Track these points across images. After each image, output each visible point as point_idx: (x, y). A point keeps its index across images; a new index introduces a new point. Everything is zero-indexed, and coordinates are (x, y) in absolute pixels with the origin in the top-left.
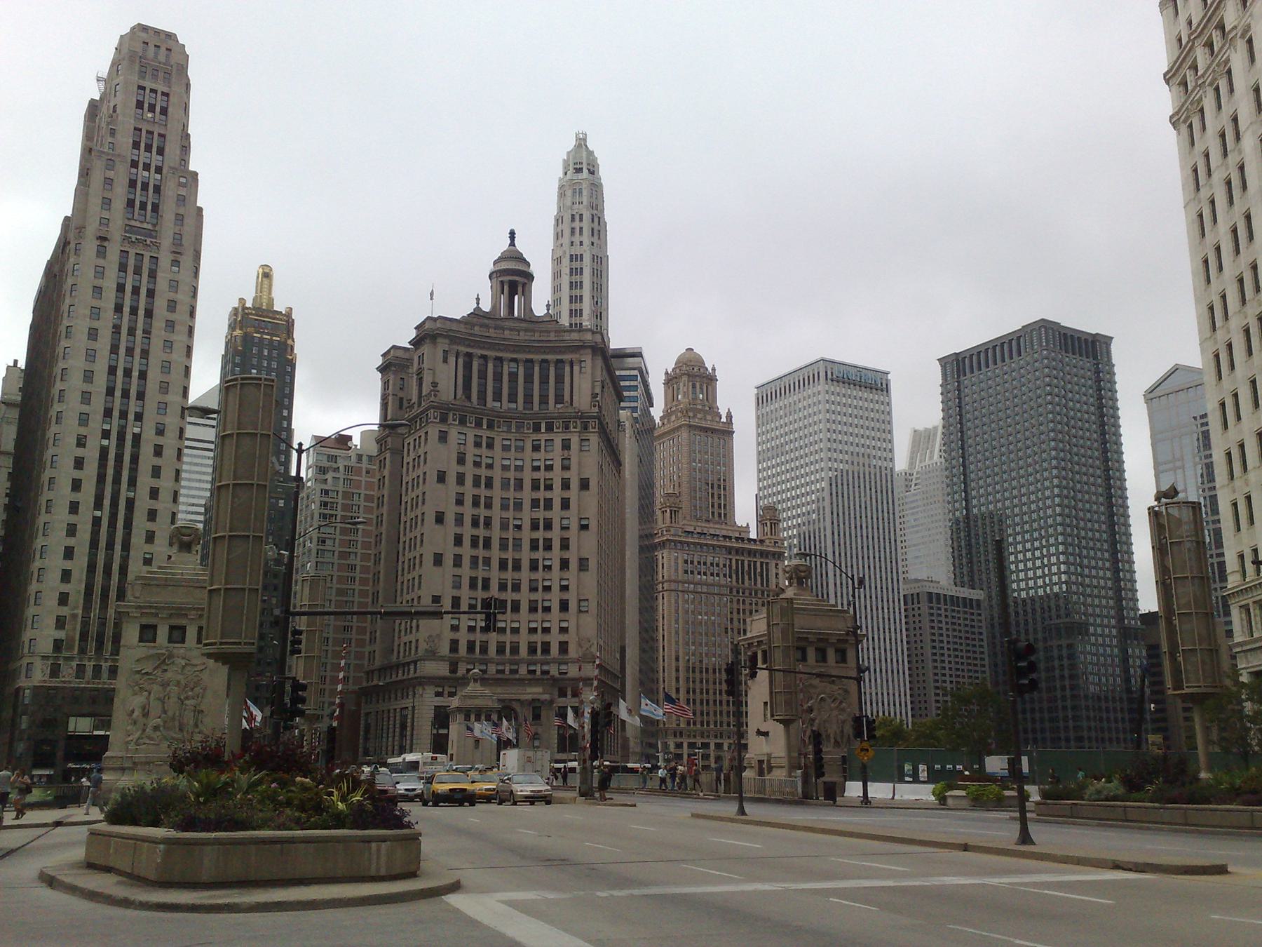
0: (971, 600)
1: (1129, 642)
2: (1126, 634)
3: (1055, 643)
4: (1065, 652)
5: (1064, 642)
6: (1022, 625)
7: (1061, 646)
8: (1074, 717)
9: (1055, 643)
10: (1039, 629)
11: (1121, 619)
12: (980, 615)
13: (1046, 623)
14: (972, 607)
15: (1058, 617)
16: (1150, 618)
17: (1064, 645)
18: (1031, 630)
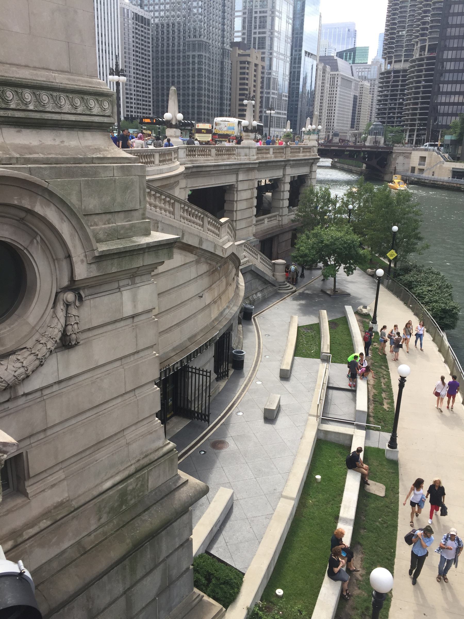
0: (145, 18)
2: (224, 53)
3: (191, 53)
4: (196, 60)
5: (196, 53)
6: (171, 40)
7: (194, 55)
9: (191, 53)
10: (182, 43)
11: (223, 43)
12: (149, 30)
13: (187, 40)
14: (145, 25)
15: (195, 36)
16: (234, 44)
17: (197, 55)
18: (176, 44)
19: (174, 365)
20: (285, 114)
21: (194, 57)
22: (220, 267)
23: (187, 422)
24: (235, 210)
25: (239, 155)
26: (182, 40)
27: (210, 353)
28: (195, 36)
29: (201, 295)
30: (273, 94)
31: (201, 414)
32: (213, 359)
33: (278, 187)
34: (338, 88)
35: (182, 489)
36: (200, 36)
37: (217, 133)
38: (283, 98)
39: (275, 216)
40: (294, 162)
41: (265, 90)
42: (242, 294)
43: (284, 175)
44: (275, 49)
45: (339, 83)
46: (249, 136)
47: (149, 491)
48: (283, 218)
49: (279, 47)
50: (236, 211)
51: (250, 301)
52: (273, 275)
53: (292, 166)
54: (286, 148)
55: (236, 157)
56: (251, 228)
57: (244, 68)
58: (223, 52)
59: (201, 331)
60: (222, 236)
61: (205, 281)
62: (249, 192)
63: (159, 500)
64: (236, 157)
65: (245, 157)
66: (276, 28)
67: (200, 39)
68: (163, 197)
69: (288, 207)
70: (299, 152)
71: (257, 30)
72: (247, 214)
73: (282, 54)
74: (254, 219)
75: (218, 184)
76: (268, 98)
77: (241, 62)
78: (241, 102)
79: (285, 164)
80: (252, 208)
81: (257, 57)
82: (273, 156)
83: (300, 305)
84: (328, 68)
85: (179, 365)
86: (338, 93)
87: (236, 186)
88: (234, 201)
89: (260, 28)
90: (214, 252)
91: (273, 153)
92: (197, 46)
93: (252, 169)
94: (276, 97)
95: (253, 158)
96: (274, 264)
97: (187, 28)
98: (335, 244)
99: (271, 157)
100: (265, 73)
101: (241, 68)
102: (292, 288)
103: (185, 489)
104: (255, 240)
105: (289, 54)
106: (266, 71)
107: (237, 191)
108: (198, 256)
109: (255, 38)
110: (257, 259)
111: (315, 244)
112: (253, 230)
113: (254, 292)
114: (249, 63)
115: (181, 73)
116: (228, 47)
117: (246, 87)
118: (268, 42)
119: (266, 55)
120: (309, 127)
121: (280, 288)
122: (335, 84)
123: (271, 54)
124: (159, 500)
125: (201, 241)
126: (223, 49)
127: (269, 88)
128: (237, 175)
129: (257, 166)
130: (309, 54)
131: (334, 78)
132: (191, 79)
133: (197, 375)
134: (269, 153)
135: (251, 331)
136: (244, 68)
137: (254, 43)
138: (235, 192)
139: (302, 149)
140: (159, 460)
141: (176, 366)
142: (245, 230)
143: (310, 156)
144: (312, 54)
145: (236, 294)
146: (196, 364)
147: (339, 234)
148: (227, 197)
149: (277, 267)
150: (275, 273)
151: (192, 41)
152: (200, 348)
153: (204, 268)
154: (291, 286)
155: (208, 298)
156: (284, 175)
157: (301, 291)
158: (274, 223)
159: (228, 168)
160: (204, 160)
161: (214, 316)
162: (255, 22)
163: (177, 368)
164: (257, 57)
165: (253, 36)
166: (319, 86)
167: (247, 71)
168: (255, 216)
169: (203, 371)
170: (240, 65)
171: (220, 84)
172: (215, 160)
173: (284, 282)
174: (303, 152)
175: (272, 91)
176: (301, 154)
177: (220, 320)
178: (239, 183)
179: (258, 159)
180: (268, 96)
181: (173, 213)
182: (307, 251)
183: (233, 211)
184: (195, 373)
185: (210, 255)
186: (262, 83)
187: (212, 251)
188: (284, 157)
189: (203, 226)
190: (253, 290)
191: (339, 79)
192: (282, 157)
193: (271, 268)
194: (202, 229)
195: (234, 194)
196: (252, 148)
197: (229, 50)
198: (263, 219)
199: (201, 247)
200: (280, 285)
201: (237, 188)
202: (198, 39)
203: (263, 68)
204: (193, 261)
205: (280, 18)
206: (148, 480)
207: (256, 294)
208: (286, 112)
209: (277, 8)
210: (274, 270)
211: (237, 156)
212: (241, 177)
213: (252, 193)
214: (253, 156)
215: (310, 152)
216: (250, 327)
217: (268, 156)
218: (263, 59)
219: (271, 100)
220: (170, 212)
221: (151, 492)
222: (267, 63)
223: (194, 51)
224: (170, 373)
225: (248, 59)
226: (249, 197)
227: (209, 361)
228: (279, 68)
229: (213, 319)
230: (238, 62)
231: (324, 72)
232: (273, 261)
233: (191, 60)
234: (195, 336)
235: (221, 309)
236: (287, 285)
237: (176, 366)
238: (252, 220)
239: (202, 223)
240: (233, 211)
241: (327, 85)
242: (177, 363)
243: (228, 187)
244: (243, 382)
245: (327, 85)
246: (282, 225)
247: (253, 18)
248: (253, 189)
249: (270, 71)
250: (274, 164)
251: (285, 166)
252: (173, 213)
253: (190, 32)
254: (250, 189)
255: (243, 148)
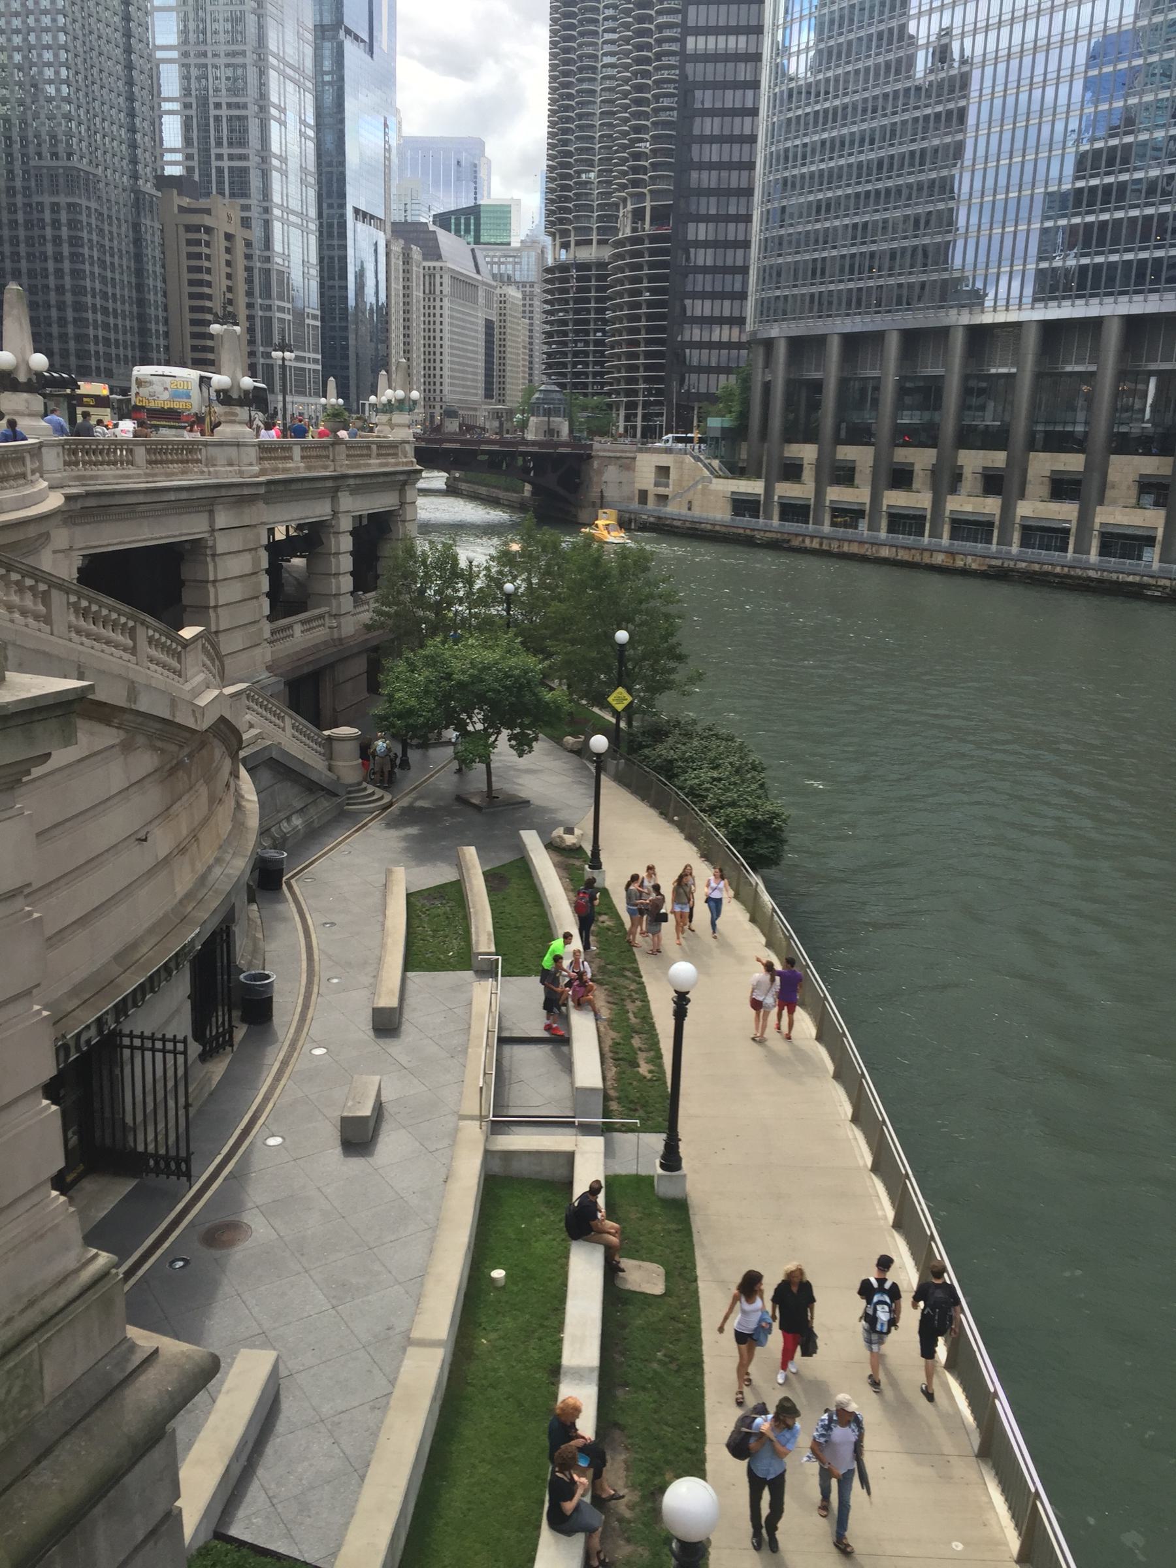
1: (142, 214)
2: (139, 201)
3: (47, 199)
5: (63, 200)
7: (58, 204)
8: (76, 320)
9: (47, 199)
10: (18, 172)
11: (135, 177)
13: (32, 163)
15: (55, 155)
16: (164, 182)
19: (78, 1035)
20: (316, 361)
21: (55, 208)
22: (190, 756)
23: (125, 1187)
24: (212, 604)
25: (210, 462)
26: (18, 164)
27: (180, 988)
28: (55, 155)
29: (142, 835)
30: (281, 309)
31: (167, 1158)
32: (188, 1006)
33: (321, 543)
34: (446, 300)
35: (143, 1378)
36: (69, 155)
37: (143, 407)
38: (307, 321)
39: (321, 617)
40: (358, 481)
41: (259, 301)
42: (253, 822)
43: (335, 513)
44: (276, 198)
45: (447, 289)
46: (236, 415)
47: (47, 1400)
48: (343, 620)
49: (285, 195)
50: (216, 607)
51: (274, 839)
52: (330, 769)
53: (355, 491)
54: (333, 444)
55: (205, 469)
56: (258, 651)
57: (198, 243)
58: (137, 199)
59: (150, 931)
60: (189, 674)
61: (152, 798)
62: (248, 557)
63: (79, 1422)
64: (205, 469)
65: (229, 468)
66: (275, 148)
67: (69, 164)
68: (15, 577)
69: (352, 593)
70: (369, 456)
71: (225, 151)
72: (246, 613)
73: (294, 213)
74: (267, 627)
75: (161, 538)
76: (268, 322)
77: (189, 228)
78: (197, 329)
79: (335, 486)
80: (257, 598)
81: (229, 217)
82: (302, 465)
83: (406, 838)
84: (416, 252)
85: (93, 1031)
86: (446, 312)
87: (210, 543)
88: (207, 582)
89: (230, 144)
90: (171, 718)
91: (303, 457)
92: (61, 180)
93: (252, 499)
94: (290, 317)
95: (252, 470)
96: (330, 738)
97: (30, 134)
98: (482, 680)
99: (296, 466)
100: (256, 258)
101: (190, 243)
102: (382, 798)
103: (151, 1375)
104: (274, 679)
105: (313, 212)
106: (258, 252)
107: (214, 555)
108: (127, 731)
109: (220, 170)
110: (284, 730)
111: (431, 681)
112: (265, 654)
113: (282, 815)
114: (209, 230)
115: (23, 249)
116: (148, 188)
117: (207, 290)
118: (255, 182)
119: (255, 213)
120: (387, 395)
121: (349, 799)
122: (438, 292)
123: (267, 210)
124: (79, 1422)
125: (133, 691)
126: (137, 192)
127: (267, 293)
128: (211, 513)
129: (262, 490)
130: (365, 214)
131: (431, 276)
132: (51, 265)
133: (148, 1054)
134: (291, 458)
135: (285, 919)
136: (198, 243)
137: (220, 182)
138: (209, 559)
139: (374, 447)
140: (71, 1308)
141: (84, 1038)
142: (244, 656)
143: (397, 464)
144: (372, 217)
145: (238, 823)
146: (142, 1022)
147: (490, 656)
148: (187, 572)
149: (336, 745)
150: (333, 763)
151: (48, 168)
152: (151, 977)
153: (145, 761)
154: (379, 793)
155: (162, 842)
156: (335, 513)
157: (405, 802)
158: (320, 634)
159: (184, 495)
160: (115, 477)
161: (181, 890)
162: (218, 129)
163: (88, 1042)
164: (229, 217)
165: (214, 163)
166: (397, 295)
167: (206, 250)
168: (268, 617)
169: (164, 1039)
170: (184, 236)
171: (133, 280)
172: (147, 475)
173: (360, 784)
174: (379, 455)
175: (278, 303)
176: (372, 461)
177: (200, 897)
178: (217, 534)
179: (263, 472)
180: (268, 314)
181: (47, 620)
182: (413, 702)
183: (208, 608)
184: (142, 1049)
185: (158, 726)
186: (249, 281)
187: (166, 715)
188: (332, 469)
189: (133, 651)
190: (278, 812)
191: (447, 280)
192: (325, 467)
193: (322, 751)
194: (133, 659)
195: (207, 564)
196: (245, 445)
197: (151, 196)
198: (290, 627)
199: (133, 707)
200: (350, 792)
201: (214, 547)
202: (63, 163)
203: (248, 244)
204: (113, 746)
205: (283, 123)
206: (41, 1371)
207: (288, 819)
208: (319, 357)
209: (274, 98)
210: (330, 756)
211: (207, 465)
212: (223, 519)
213: (256, 561)
214: (251, 465)
215: (395, 455)
216: (280, 907)
217: (290, 465)
218: (246, 223)
219: (276, 326)
220: (37, 617)
221: (54, 1401)
222: (257, 233)
223: (55, 192)
224: (67, 1056)
225: (207, 221)
226: (248, 569)
227: (178, 1011)
228: (292, 247)
229: (180, 895)
230: (181, 229)
231: (407, 259)
232: (327, 733)
233: (47, 216)
234: (134, 946)
235: (200, 868)
236: (369, 791)
237: (84, 1038)
238: (261, 629)
239: (130, 643)
240: (208, 608)
241: (417, 293)
242: (88, 1027)
243: (188, 546)
244: (274, 1057)
245: (417, 293)
246: (340, 639)
247: (212, 120)
248: (256, 549)
249: (266, 254)
250: (306, 485)
251: (337, 489)
252: (47, 620)
253: (39, 145)
254: (250, 550)
255: (221, 444)
